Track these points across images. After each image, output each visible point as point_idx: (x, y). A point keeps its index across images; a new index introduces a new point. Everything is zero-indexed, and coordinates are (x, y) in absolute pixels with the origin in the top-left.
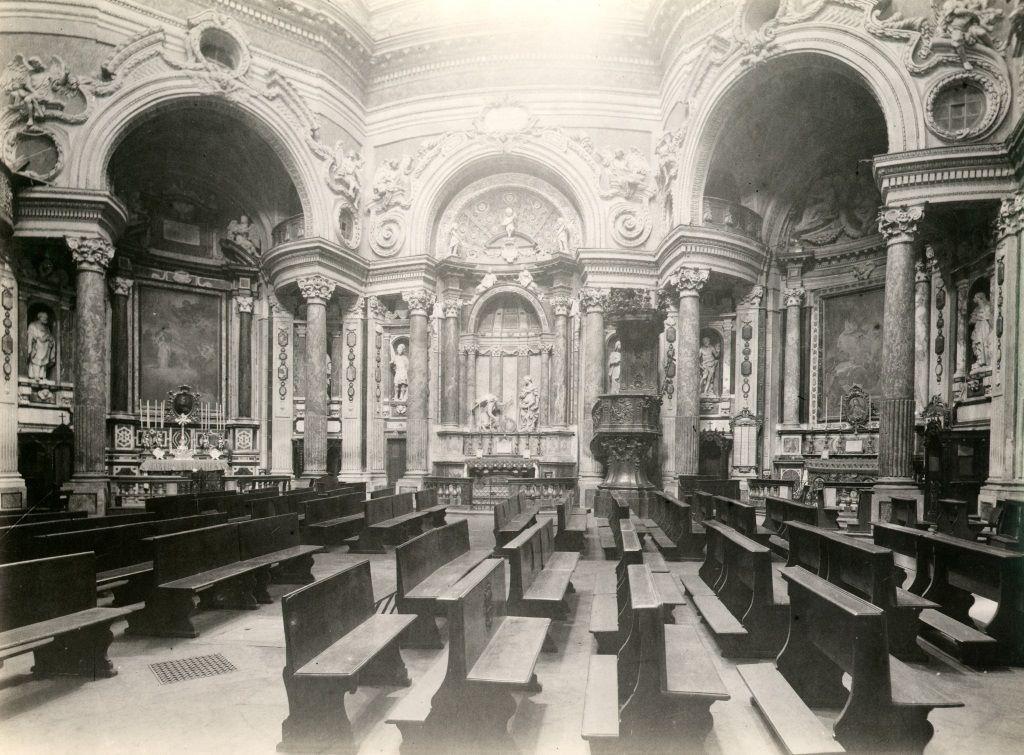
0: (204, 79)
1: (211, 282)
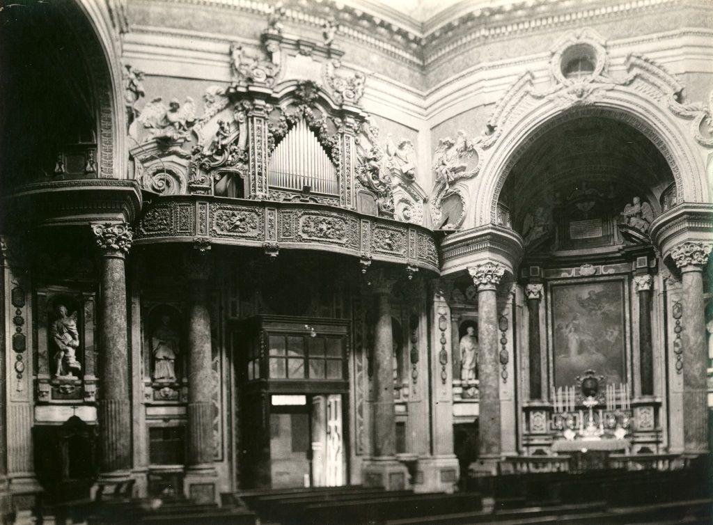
0: (563, 96)
1: (614, 268)
